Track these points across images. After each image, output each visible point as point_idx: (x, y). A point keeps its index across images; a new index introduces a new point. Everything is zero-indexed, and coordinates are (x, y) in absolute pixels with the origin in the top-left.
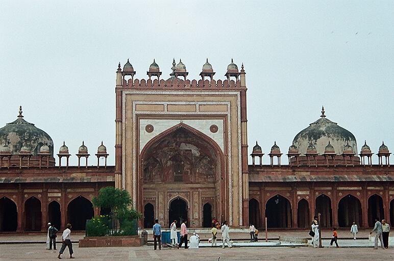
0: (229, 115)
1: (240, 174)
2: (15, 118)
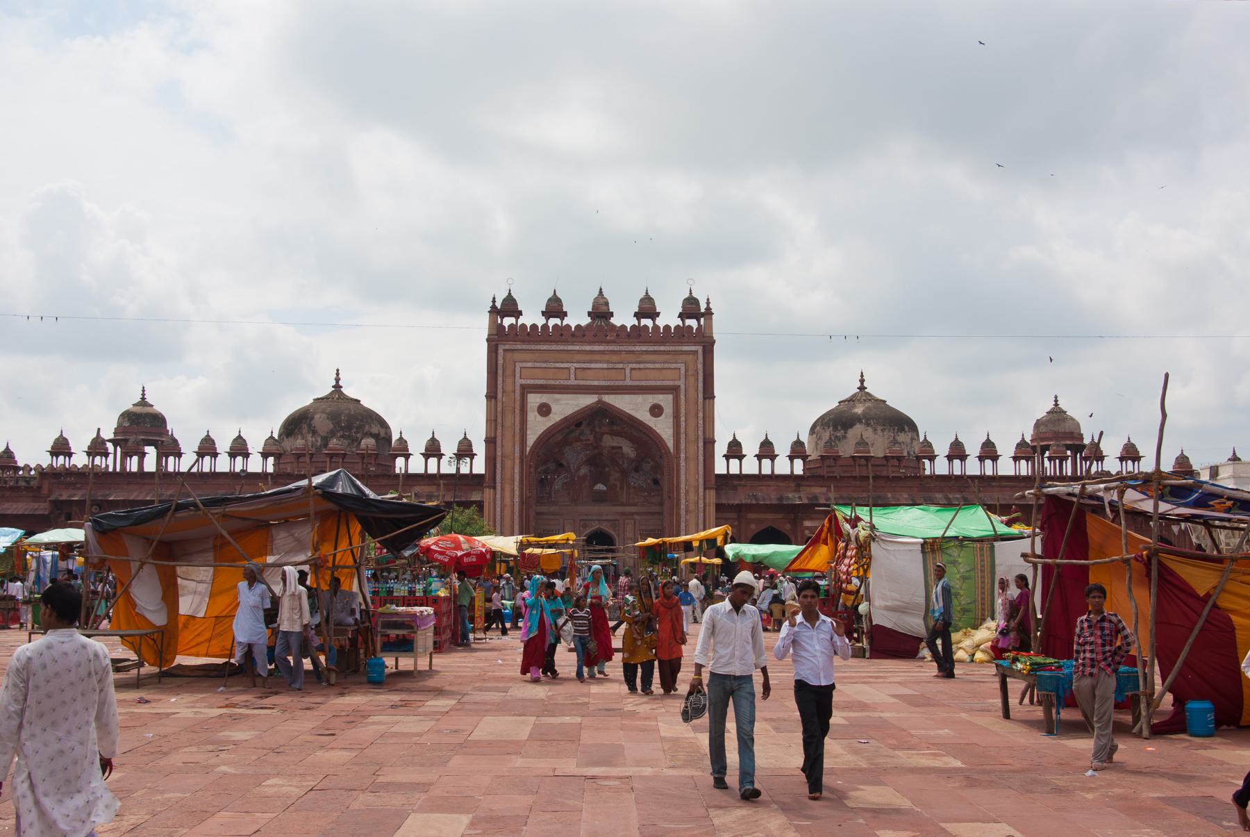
0: (683, 387)
1: (701, 490)
2: (326, 390)
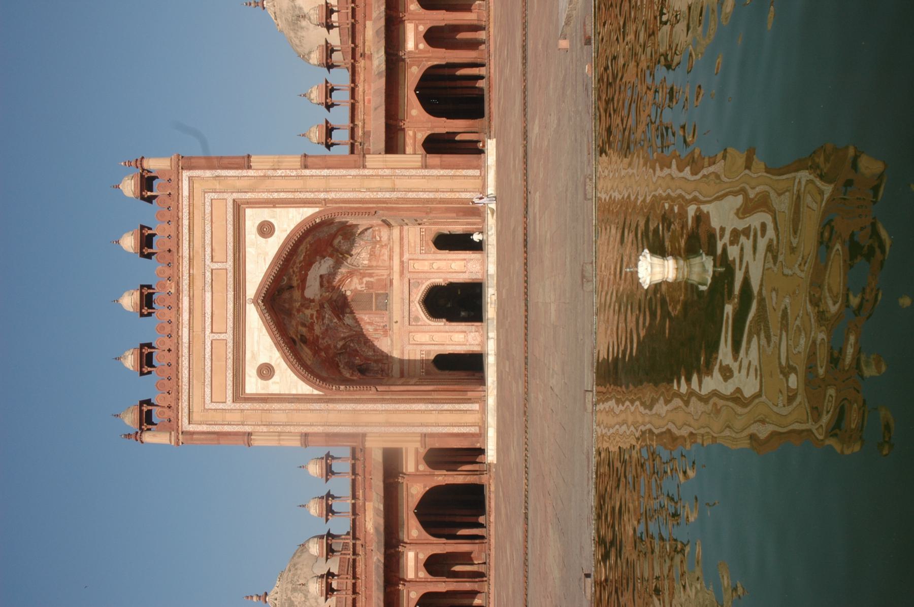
1: (366, 172)
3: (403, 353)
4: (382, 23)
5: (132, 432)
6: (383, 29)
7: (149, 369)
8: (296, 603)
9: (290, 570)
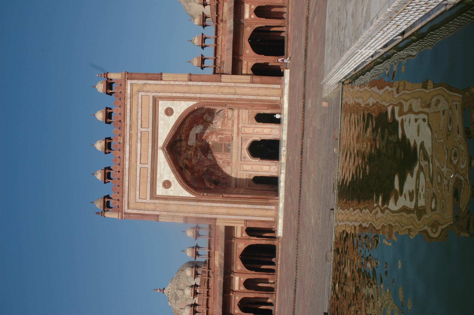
3: (237, 175)
4: (232, 4)
5: (100, 212)
6: (233, 8)
7: (109, 180)
8: (179, 296)
9: (176, 279)
